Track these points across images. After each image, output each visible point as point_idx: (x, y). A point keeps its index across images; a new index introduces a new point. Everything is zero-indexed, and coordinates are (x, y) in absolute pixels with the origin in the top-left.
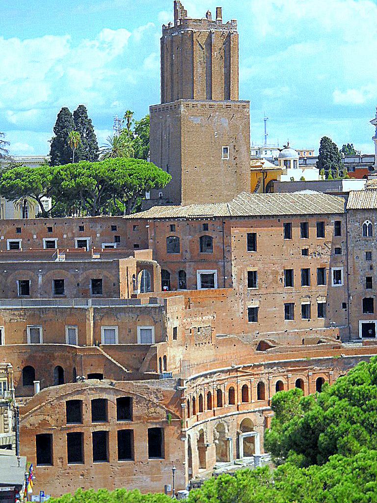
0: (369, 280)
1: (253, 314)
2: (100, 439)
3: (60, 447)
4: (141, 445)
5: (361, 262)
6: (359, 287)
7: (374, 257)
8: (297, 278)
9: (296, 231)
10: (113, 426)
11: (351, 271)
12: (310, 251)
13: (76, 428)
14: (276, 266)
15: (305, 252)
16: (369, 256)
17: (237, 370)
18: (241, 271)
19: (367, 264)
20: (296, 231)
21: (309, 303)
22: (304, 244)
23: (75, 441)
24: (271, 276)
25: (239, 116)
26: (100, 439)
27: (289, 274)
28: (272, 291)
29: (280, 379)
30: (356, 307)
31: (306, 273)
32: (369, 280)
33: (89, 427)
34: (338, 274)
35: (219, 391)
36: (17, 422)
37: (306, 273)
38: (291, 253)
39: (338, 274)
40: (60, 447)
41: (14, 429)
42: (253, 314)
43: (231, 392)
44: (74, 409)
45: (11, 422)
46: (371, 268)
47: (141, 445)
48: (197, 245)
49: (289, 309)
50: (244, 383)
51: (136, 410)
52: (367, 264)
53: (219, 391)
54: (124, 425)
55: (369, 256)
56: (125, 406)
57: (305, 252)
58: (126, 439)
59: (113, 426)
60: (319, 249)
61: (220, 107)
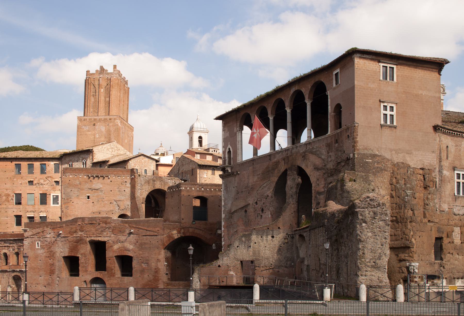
12: (35, 182)
14: (9, 191)
15: (31, 182)
21: (33, 216)
24: (4, 198)
25: (112, 124)
28: (5, 206)
38: (20, 183)
57: (31, 182)
60: (42, 181)
61: (100, 120)
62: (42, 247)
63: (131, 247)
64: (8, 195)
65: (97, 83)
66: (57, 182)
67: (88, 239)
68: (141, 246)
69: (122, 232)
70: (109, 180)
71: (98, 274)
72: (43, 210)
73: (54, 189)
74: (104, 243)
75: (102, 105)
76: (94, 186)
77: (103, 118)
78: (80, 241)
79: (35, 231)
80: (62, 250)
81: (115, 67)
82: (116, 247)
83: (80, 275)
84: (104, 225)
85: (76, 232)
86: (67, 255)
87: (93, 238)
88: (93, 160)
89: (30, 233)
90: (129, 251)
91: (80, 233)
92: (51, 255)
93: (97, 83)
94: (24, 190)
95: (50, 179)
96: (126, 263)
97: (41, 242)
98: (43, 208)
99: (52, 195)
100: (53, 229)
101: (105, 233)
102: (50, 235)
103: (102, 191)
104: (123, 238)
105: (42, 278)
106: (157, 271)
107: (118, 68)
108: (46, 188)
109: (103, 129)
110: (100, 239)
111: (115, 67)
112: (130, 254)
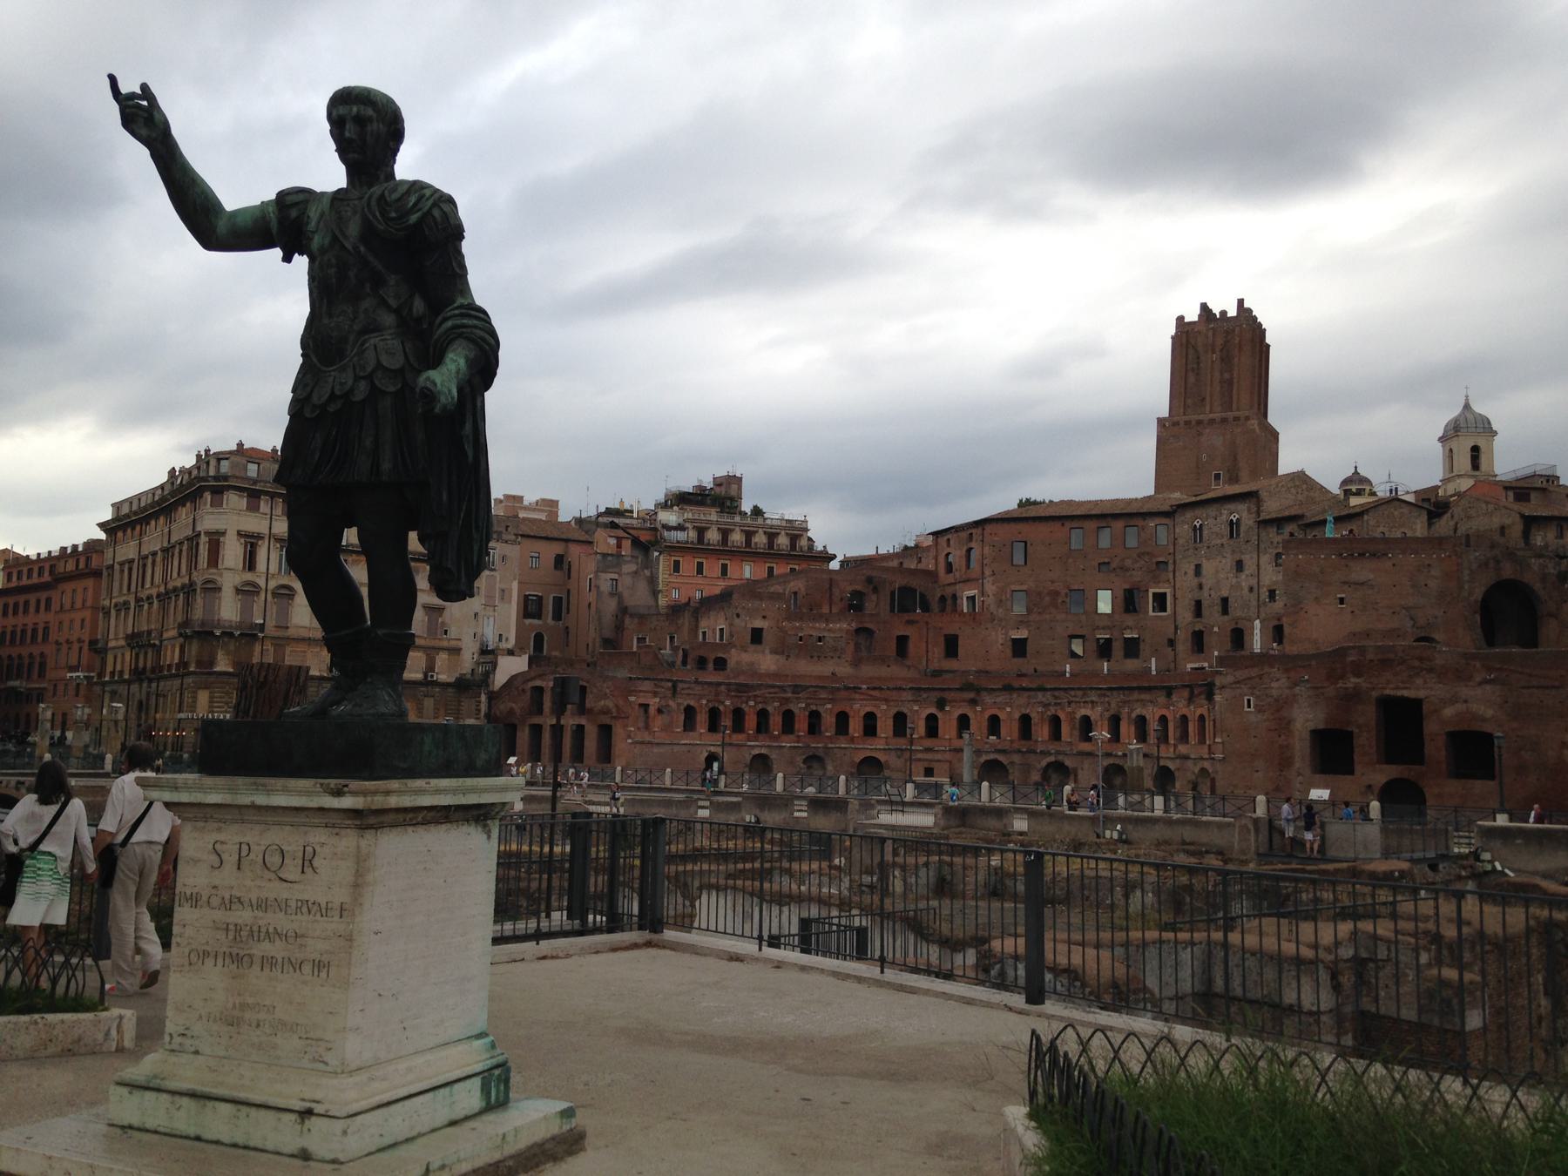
0: (1198, 604)
5: (1190, 580)
6: (1186, 616)
7: (1204, 572)
11: (1179, 595)
12: (1113, 565)
13: (536, 720)
16: (1198, 568)
17: (855, 689)
19: (1196, 581)
24: (1047, 599)
29: (933, 710)
30: (1183, 646)
32: (1198, 604)
36: (490, 707)
41: (487, 716)
42: (1019, 647)
46: (1201, 587)
50: (868, 709)
52: (1196, 581)
55: (1198, 568)
60: (1128, 563)
61: (1212, 421)
62: (1259, 710)
63: (1490, 713)
67: (1374, 694)
70: (1389, 564)
72: (1130, 623)
73: (1157, 583)
74: (1418, 703)
76: (1354, 577)
78: (1352, 698)
79: (1240, 674)
80: (1306, 718)
81: (1241, 302)
82: (1448, 712)
83: (1358, 768)
84: (1417, 663)
85: (1342, 677)
86: (1321, 727)
87: (1387, 692)
88: (1259, 515)
89: (1230, 679)
90: (1484, 720)
91: (1353, 680)
92: (1283, 726)
95: (1146, 558)
97: (1257, 697)
98: (1130, 620)
99: (1151, 591)
100: (1287, 671)
101: (1419, 681)
102: (1278, 684)
103: (1372, 587)
104: (1465, 692)
105: (1260, 774)
107: (1246, 305)
108: (1137, 576)
110: (1406, 693)
111: (1241, 302)
112: (1487, 728)
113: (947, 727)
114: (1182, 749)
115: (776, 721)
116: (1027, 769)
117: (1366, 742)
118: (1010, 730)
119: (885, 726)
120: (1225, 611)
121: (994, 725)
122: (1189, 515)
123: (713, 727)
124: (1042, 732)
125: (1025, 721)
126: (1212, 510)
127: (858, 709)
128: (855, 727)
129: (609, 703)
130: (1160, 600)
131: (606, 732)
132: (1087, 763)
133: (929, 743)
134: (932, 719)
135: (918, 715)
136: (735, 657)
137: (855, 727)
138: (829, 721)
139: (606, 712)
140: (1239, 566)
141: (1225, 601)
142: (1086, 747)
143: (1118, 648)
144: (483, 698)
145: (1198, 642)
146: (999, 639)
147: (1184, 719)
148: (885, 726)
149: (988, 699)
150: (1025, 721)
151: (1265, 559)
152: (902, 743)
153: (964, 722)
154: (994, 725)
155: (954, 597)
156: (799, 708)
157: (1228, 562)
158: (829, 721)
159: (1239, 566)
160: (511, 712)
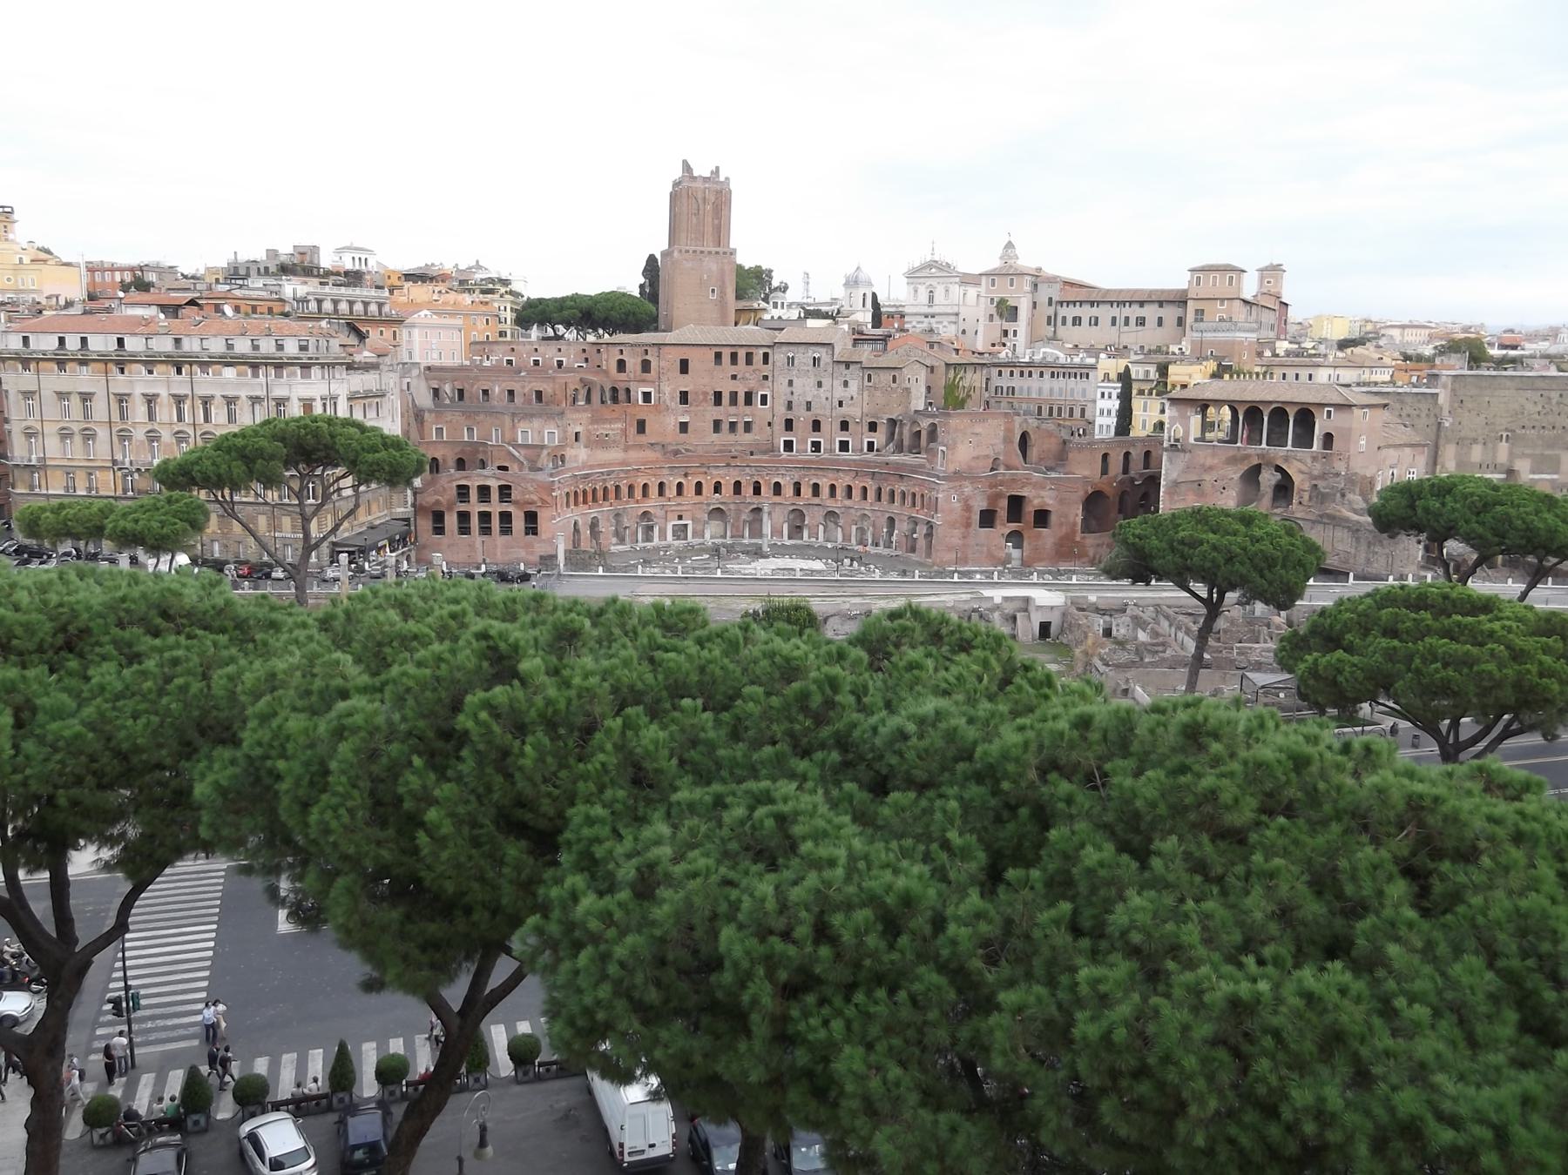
0: (790, 403)
1: (684, 427)
2: (485, 517)
3: (451, 521)
4: (518, 523)
6: (781, 410)
8: (726, 399)
9: (726, 358)
10: (495, 507)
13: (463, 507)
15: (734, 377)
16: (791, 383)
18: (674, 390)
20: (726, 358)
22: (733, 370)
23: (464, 517)
26: (485, 517)
27: (718, 396)
30: (779, 425)
31: (734, 395)
32: (790, 403)
33: (475, 507)
34: (764, 398)
35: (617, 487)
37: (734, 395)
39: (764, 398)
40: (451, 521)
41: (414, 505)
42: (684, 427)
43: (631, 488)
44: (463, 492)
45: (410, 499)
47: (518, 523)
48: (639, 368)
49: (717, 425)
51: (515, 495)
53: (617, 487)
54: (506, 507)
55: (791, 383)
56: (505, 491)
57: (734, 377)
58: (506, 517)
59: (495, 507)
64: (705, 394)
65: (700, 196)
66: (766, 378)
68: (1061, 501)
69: (1043, 488)
71: (1014, 526)
73: (763, 387)
75: (709, 229)
77: (714, 250)
78: (999, 496)
80: (980, 504)
82: (1036, 502)
93: (700, 196)
94: (726, 388)
96: (1042, 517)
98: (748, 409)
104: (1043, 493)
106: (1075, 524)
108: (752, 384)
109: (714, 267)
113: (689, 489)
114: (848, 503)
115: (600, 494)
116: (739, 512)
117: (1002, 513)
118: (728, 490)
119: (654, 491)
120: (809, 409)
121: (717, 488)
122: (784, 348)
123: (576, 504)
124: (748, 490)
125: (738, 485)
126: (801, 349)
127: (641, 481)
128: (638, 493)
129: (534, 498)
130: (764, 399)
131: (531, 518)
132: (777, 508)
133: (679, 500)
134: (680, 485)
135: (672, 482)
136: (569, 453)
137: (638, 493)
138: (625, 490)
139: (532, 503)
140: (820, 384)
141: (809, 404)
142: (777, 499)
143: (741, 427)
144: (409, 492)
145: (789, 424)
146: (671, 422)
147: (850, 487)
148: (654, 491)
149: (715, 472)
150: (738, 485)
151: (838, 384)
152: (662, 501)
153: (699, 485)
154: (717, 488)
155: (628, 391)
156: (610, 485)
157: (812, 381)
158: (625, 490)
159: (820, 384)
160: (438, 502)
